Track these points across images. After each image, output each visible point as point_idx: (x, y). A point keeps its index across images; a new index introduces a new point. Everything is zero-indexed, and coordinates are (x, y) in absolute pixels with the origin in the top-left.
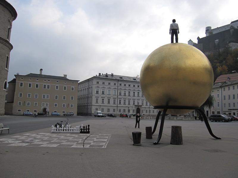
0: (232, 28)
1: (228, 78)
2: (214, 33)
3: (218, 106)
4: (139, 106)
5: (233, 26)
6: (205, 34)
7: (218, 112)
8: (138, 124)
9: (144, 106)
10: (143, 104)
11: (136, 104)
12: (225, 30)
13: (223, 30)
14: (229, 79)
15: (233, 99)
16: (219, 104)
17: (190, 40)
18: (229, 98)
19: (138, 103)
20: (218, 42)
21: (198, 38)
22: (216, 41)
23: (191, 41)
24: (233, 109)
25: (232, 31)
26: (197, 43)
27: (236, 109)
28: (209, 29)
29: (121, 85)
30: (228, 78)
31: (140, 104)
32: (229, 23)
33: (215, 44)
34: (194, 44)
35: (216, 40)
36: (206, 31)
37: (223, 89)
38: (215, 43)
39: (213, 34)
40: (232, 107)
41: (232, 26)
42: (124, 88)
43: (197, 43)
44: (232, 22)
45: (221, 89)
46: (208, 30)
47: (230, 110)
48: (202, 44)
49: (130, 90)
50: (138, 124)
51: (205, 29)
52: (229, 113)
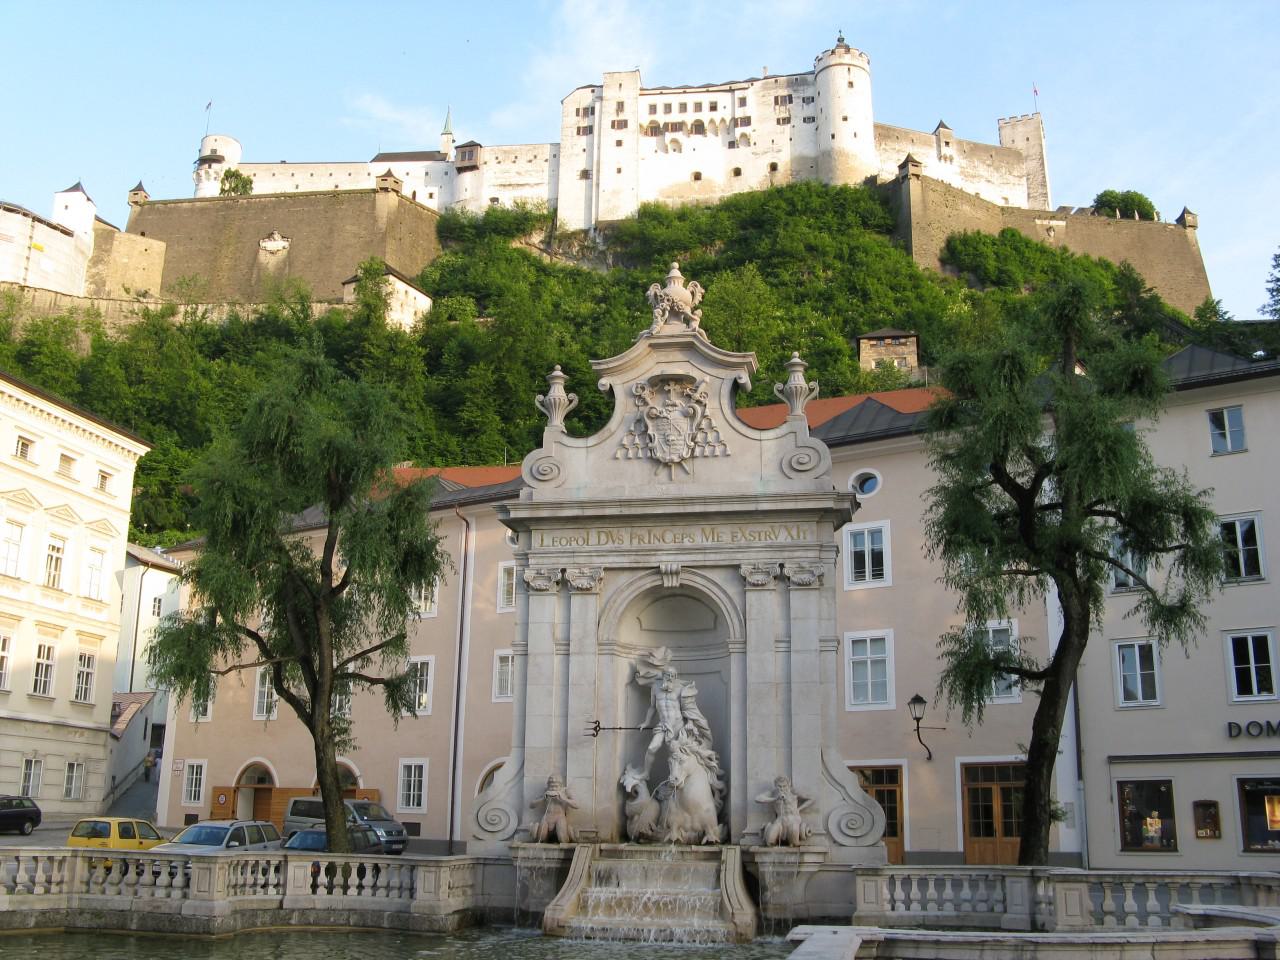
2: (260, 188)
7: (970, 771)
20: (283, 254)
22: (269, 245)
23: (78, 194)
35: (270, 236)
38: (263, 257)
39: (254, 192)
41: (389, 174)
44: (382, 158)
48: (158, 247)
52: (1242, 782)
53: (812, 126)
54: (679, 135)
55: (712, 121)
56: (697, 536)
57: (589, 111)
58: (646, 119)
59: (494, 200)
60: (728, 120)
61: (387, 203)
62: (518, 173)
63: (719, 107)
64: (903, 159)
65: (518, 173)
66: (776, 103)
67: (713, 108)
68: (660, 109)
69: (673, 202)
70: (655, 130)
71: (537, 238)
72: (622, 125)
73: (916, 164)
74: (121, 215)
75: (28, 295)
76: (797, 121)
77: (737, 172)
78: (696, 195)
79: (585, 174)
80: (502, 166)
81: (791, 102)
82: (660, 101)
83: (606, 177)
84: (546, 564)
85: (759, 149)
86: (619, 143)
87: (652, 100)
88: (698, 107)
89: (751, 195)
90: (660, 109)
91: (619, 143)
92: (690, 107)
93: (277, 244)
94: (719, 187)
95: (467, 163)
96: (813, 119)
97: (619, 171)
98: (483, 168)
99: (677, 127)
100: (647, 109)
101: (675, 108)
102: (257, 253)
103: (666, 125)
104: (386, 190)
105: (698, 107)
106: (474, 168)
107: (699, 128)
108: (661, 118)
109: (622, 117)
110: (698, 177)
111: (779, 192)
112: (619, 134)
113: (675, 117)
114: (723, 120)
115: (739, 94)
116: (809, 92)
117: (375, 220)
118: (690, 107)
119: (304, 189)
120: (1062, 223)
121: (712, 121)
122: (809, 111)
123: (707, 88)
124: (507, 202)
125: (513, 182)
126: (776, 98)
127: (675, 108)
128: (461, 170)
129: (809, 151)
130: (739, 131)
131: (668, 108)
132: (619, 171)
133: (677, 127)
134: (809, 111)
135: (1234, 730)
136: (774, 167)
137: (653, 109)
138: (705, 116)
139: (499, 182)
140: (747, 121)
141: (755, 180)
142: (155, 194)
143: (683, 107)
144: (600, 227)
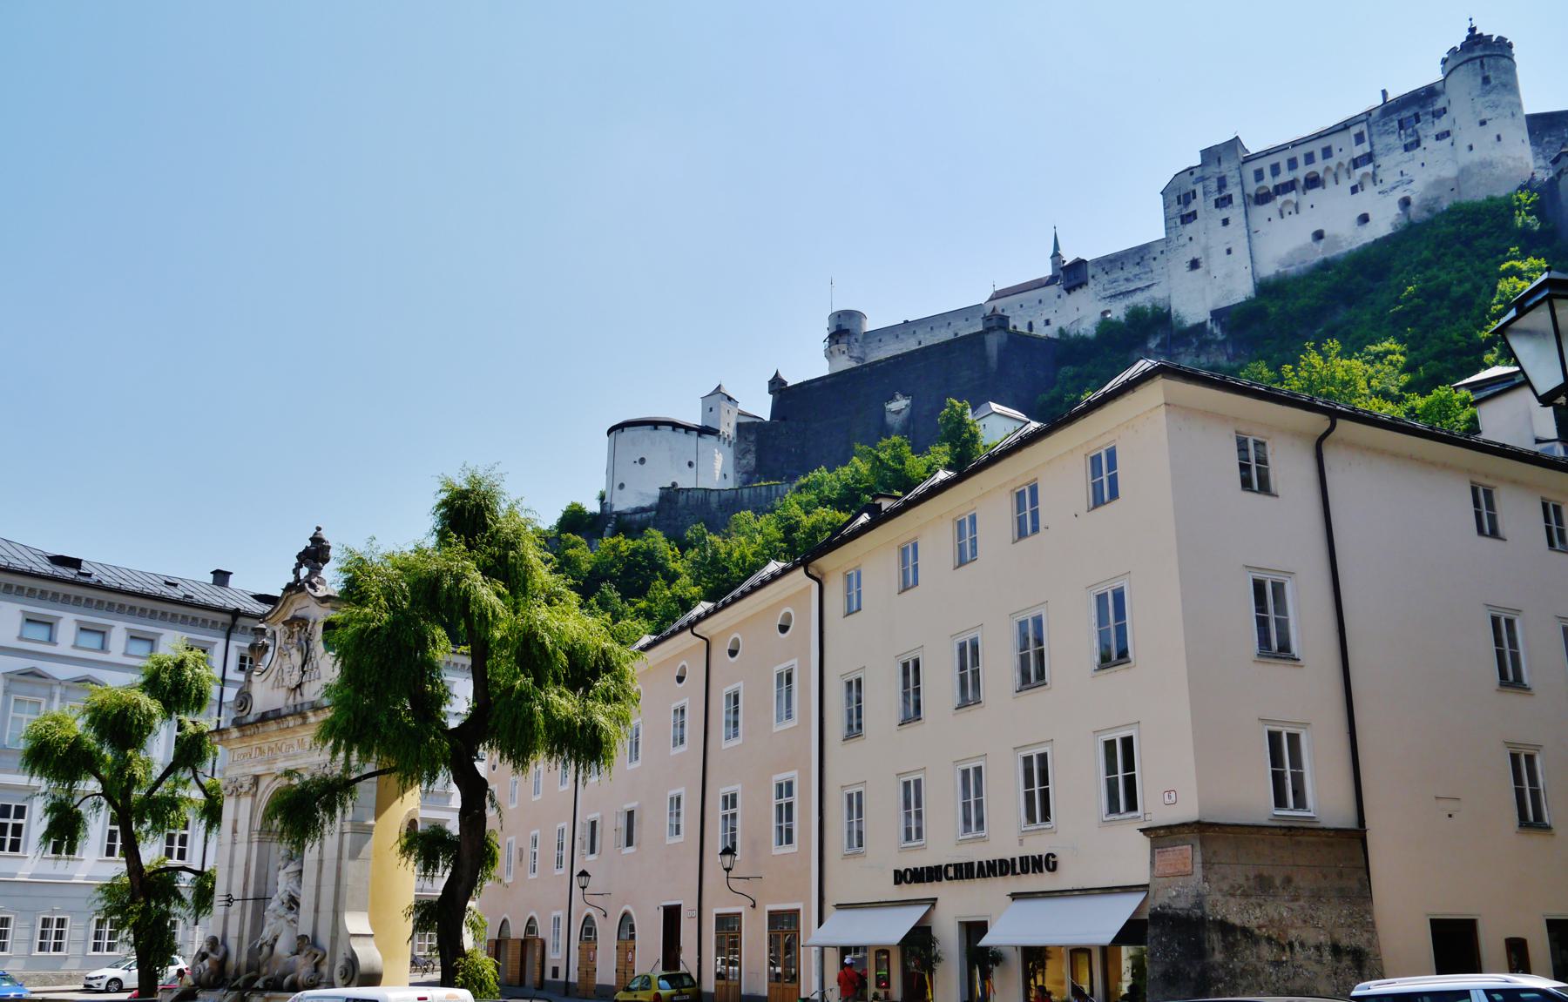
0: (994, 323)
3: (787, 836)
16: (795, 799)
21: (776, 385)
22: (894, 406)
24: (965, 871)
25: (993, 342)
26: (767, 418)
28: (846, 326)
34: (744, 420)
35: (892, 399)
38: (890, 419)
43: (766, 414)
44: (998, 295)
53: (1448, 141)
54: (1292, 196)
55: (1328, 169)
58: (1252, 187)
59: (1104, 313)
60: (1346, 162)
61: (993, 342)
62: (1127, 280)
63: (1335, 151)
65: (1127, 280)
66: (1401, 127)
67: (1327, 153)
68: (1267, 173)
70: (1263, 198)
72: (1224, 202)
74: (762, 407)
75: (682, 498)
76: (1428, 142)
78: (1319, 253)
79: (1194, 264)
80: (1113, 276)
81: (1418, 121)
82: (1265, 164)
83: (1217, 263)
86: (1226, 222)
87: (1256, 165)
88: (1310, 158)
89: (1386, 239)
90: (1267, 173)
92: (1301, 161)
93: (900, 404)
94: (1349, 237)
95: (1074, 282)
96: (1448, 134)
97: (1229, 251)
98: (1091, 282)
99: (1289, 186)
101: (1284, 166)
102: (883, 417)
103: (1276, 188)
105: (1310, 158)
106: (1082, 284)
107: (1313, 182)
108: (1269, 182)
109: (1226, 193)
110: (1319, 235)
112: (1225, 213)
113: (1285, 176)
114: (1340, 164)
115: (1355, 130)
117: (984, 358)
118: (1301, 161)
121: (1328, 169)
123: (1320, 136)
124: (1118, 312)
125: (1123, 289)
126: (1400, 122)
127: (1284, 166)
128: (1069, 290)
129: (1449, 172)
130: (1359, 172)
131: (1275, 170)
132: (1229, 251)
133: (1289, 186)
134: (1442, 124)
135: (900, 877)
136: (1405, 203)
137: (1259, 175)
138: (1319, 167)
139: (1112, 292)
140: (1369, 158)
141: (1384, 222)
142: (792, 380)
143: (1292, 164)
144: (1217, 314)
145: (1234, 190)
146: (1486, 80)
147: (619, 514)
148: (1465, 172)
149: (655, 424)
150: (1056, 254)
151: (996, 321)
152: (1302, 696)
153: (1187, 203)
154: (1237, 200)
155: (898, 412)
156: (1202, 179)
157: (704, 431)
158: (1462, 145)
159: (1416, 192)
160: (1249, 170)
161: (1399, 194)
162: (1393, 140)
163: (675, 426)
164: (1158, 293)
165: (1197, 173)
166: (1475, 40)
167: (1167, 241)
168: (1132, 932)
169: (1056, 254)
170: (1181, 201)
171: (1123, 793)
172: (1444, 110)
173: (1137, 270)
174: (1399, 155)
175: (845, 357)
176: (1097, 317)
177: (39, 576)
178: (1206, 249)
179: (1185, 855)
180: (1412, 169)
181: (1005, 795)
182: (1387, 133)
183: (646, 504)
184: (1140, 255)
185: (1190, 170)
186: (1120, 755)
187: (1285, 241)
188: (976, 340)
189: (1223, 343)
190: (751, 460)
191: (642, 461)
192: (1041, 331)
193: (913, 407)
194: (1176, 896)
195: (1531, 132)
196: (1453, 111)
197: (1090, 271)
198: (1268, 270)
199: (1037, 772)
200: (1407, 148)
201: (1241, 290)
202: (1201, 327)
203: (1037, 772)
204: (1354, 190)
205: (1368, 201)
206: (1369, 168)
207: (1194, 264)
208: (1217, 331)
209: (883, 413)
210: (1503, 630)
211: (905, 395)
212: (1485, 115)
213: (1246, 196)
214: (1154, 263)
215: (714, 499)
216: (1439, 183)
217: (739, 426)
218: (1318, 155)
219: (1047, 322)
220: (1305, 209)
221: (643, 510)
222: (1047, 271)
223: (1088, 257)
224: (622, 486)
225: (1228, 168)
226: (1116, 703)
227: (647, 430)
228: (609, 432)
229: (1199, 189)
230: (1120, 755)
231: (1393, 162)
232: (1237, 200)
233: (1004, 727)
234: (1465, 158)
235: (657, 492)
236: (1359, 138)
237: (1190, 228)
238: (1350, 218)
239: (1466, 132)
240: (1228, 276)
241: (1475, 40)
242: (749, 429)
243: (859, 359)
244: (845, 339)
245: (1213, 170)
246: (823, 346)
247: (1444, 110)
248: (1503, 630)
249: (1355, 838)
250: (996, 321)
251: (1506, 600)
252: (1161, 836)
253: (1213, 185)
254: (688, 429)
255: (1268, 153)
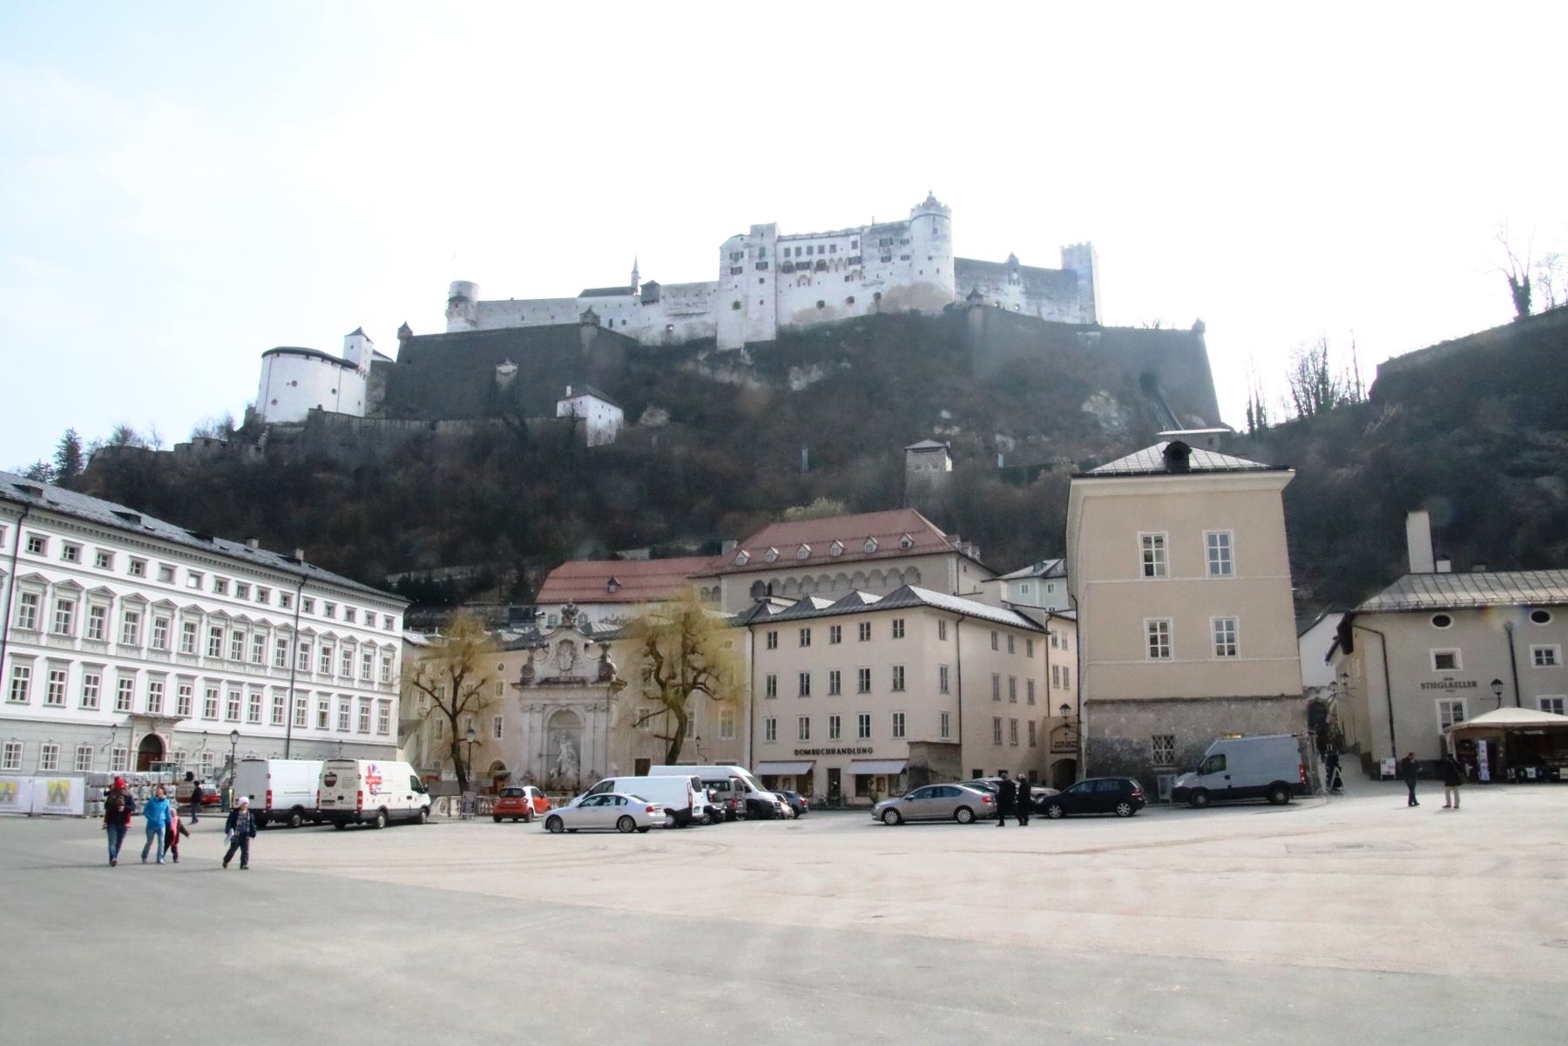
1: (612, 582)
4: (153, 721)
5: (595, 310)
6: (445, 320)
8: (238, 853)
9: (195, 721)
10: (184, 706)
11: (140, 705)
12: (549, 322)
13: (542, 323)
14: (613, 588)
15: (832, 693)
17: (359, 332)
18: (805, 690)
19: (155, 701)
20: (512, 376)
21: (404, 333)
24: (831, 752)
25: (588, 333)
27: (850, 751)
29: (37, 545)
30: (612, 582)
31: (169, 708)
32: (574, 293)
33: (493, 384)
35: (502, 362)
36: (452, 300)
37: (762, 638)
38: (499, 378)
40: (820, 737)
42: (65, 577)
44: (588, 293)
45: (749, 635)
46: (459, 299)
47: (807, 752)
49: (72, 586)
50: (238, 853)
51: (448, 289)
53: (907, 263)
54: (807, 273)
56: (572, 694)
57: (736, 256)
58: (782, 260)
61: (588, 333)
64: (969, 291)
66: (881, 243)
67: (833, 248)
68: (793, 252)
69: (802, 325)
70: (787, 269)
71: (702, 357)
72: (762, 266)
73: (981, 296)
74: (391, 349)
75: (328, 419)
76: (897, 260)
77: (851, 300)
78: (820, 318)
79: (737, 306)
83: (753, 306)
84: (530, 702)
85: (867, 282)
86: (762, 281)
88: (821, 250)
89: (862, 318)
90: (793, 252)
91: (762, 281)
92: (816, 250)
93: (508, 368)
99: (806, 266)
100: (781, 252)
101: (804, 250)
104: (584, 324)
105: (821, 250)
107: (821, 266)
108: (793, 259)
110: (821, 304)
111: (879, 315)
112: (762, 274)
113: (804, 258)
115: (852, 238)
116: (906, 236)
118: (816, 250)
119: (528, 323)
120: (1098, 334)
122: (905, 250)
123: (829, 235)
124: (680, 330)
125: (685, 310)
127: (804, 250)
128: (644, 303)
129: (906, 283)
130: (852, 268)
133: (806, 266)
134: (905, 250)
135: (797, 752)
136: (878, 296)
138: (826, 257)
140: (859, 260)
141: (862, 308)
142: (417, 331)
144: (749, 346)
145: (770, 259)
146: (935, 231)
147: (272, 426)
148: (915, 287)
149: (308, 354)
150: (635, 272)
151: (590, 318)
152: (947, 703)
153: (736, 260)
154: (771, 267)
155: (507, 374)
156: (748, 246)
157: (347, 365)
158: (917, 268)
159: (884, 290)
160: (782, 246)
161: (873, 290)
162: (875, 252)
163: (325, 357)
164: (708, 319)
165: (746, 240)
166: (931, 203)
167: (719, 284)
168: (904, 771)
169: (635, 272)
170: (733, 259)
171: (899, 730)
172: (907, 242)
173: (696, 300)
174: (877, 262)
175: (462, 319)
176: (663, 328)
177: (111, 526)
178: (746, 297)
179: (924, 750)
180: (885, 275)
181: (850, 728)
182: (870, 245)
183: (295, 419)
184: (699, 290)
185: (741, 237)
186: (899, 720)
187: (801, 302)
188: (572, 330)
189: (751, 367)
190: (381, 393)
191: (294, 383)
192: (619, 329)
193: (519, 372)
194: (918, 762)
195: (956, 269)
196: (914, 244)
197: (662, 293)
198: (786, 321)
199: (865, 721)
200: (883, 260)
201: (768, 334)
202: (735, 353)
203: (865, 721)
204: (847, 279)
205: (854, 288)
206: (858, 267)
207: (737, 306)
208: (748, 357)
209: (494, 373)
210: (996, 678)
211: (513, 362)
212: (933, 253)
213: (777, 265)
214: (708, 299)
215: (355, 424)
216: (899, 288)
217: (373, 363)
218: (827, 248)
219: (624, 322)
220: (815, 282)
221: (293, 425)
222: (627, 283)
223: (663, 281)
224: (275, 402)
225: (767, 243)
226: (898, 702)
227: (300, 360)
228: (265, 355)
229: (746, 252)
230: (899, 720)
231: (873, 267)
232: (771, 267)
233: (851, 704)
234: (919, 279)
235: (306, 411)
236: (854, 245)
237: (736, 279)
238: (838, 297)
239: (920, 263)
240: (760, 320)
241: (931, 203)
242: (380, 367)
243: (473, 323)
244: (462, 306)
245: (757, 240)
246: (446, 306)
247: (907, 242)
248: (996, 678)
249: (958, 747)
250: (590, 318)
251: (996, 671)
252: (912, 744)
253: (757, 253)
254: (334, 361)
255: (794, 238)
